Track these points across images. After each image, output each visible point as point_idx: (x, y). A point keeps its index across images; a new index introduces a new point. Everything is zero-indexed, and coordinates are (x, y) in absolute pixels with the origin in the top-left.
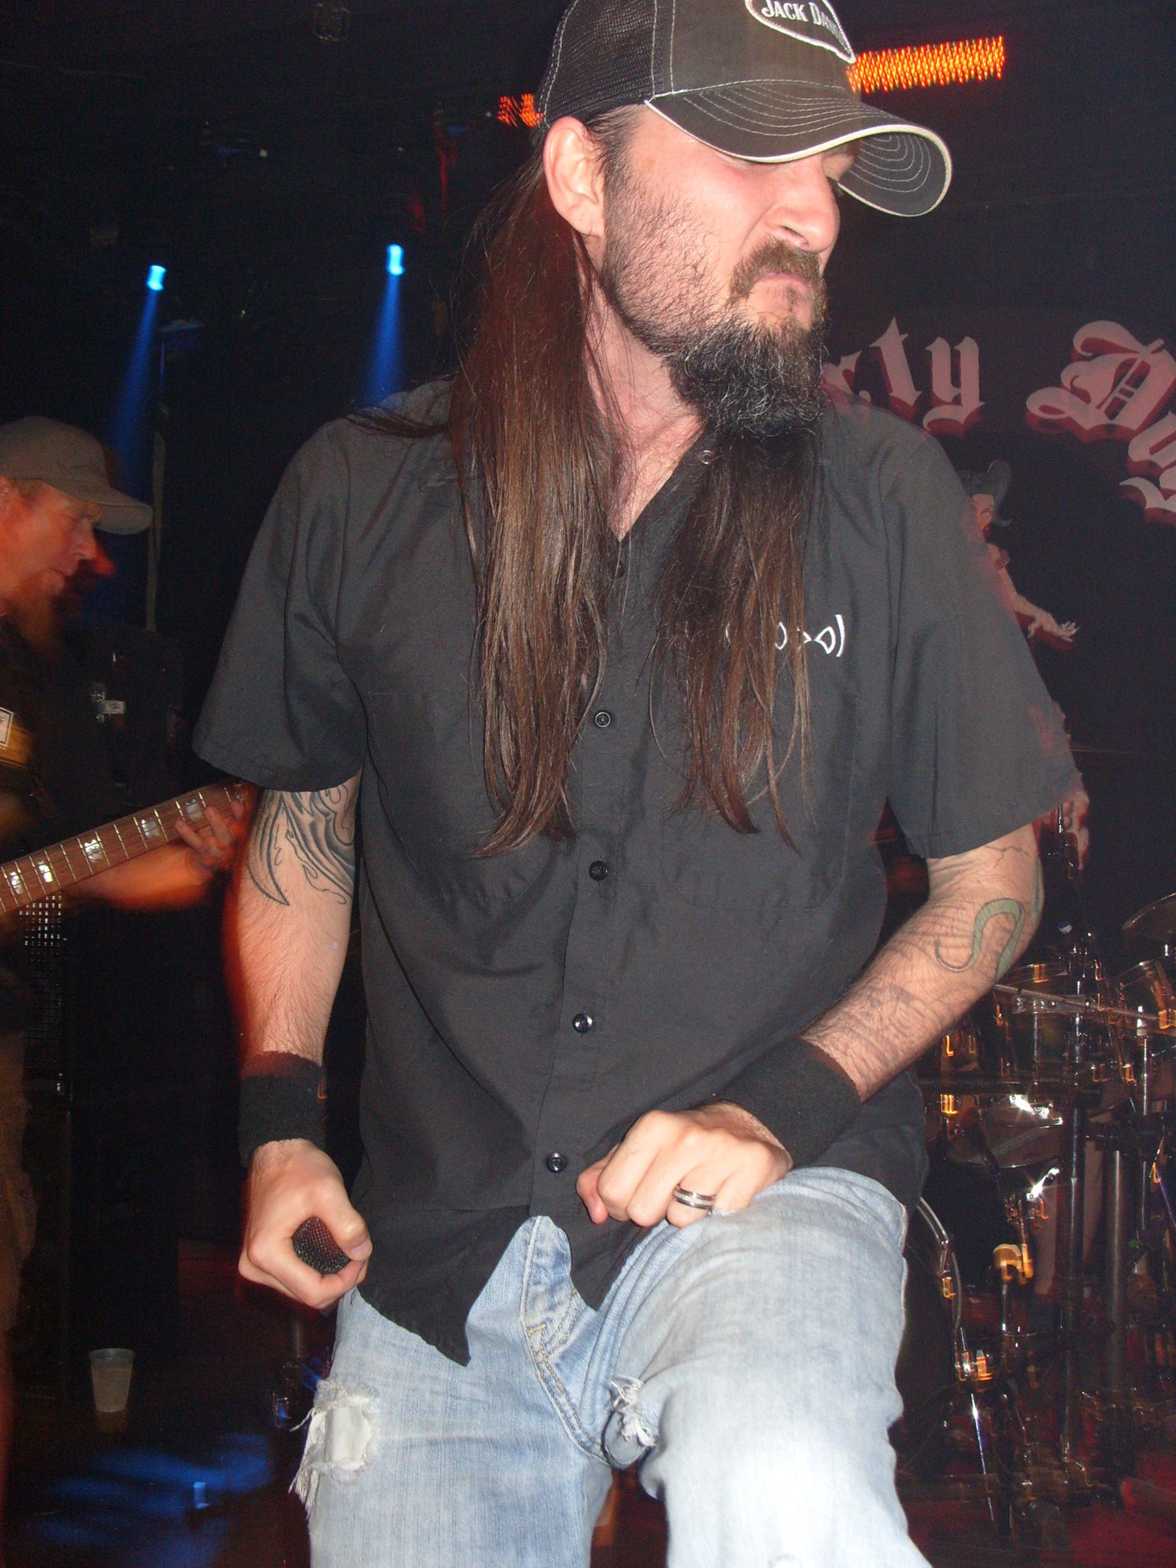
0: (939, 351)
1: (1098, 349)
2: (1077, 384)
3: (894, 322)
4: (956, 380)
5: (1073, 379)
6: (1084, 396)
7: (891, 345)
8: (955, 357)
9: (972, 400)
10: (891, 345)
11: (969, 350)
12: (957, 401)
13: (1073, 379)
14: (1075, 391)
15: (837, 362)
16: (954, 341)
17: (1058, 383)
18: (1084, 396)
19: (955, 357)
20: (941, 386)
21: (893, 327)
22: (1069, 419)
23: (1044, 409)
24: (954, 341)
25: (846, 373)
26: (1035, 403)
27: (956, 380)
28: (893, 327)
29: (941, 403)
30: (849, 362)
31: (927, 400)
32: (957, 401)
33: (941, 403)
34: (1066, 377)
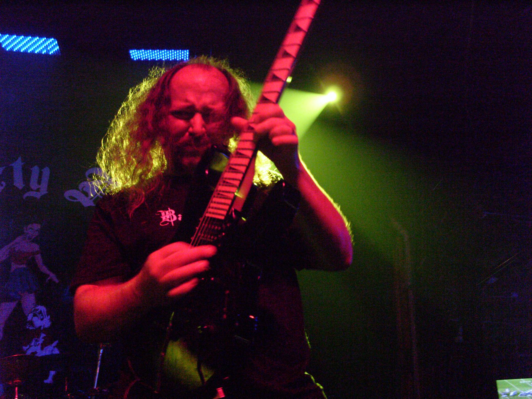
0: (35, 169)
2: (84, 189)
3: (20, 158)
4: (39, 182)
5: (84, 187)
7: (18, 165)
8: (41, 174)
9: (44, 190)
11: (46, 172)
12: (38, 190)
13: (84, 187)
16: (41, 167)
17: (77, 188)
19: (41, 174)
20: (33, 184)
21: (20, 158)
22: (79, 203)
24: (41, 167)
26: (68, 194)
27: (39, 182)
29: (32, 190)
31: (27, 188)
33: (32, 190)
34: (80, 186)
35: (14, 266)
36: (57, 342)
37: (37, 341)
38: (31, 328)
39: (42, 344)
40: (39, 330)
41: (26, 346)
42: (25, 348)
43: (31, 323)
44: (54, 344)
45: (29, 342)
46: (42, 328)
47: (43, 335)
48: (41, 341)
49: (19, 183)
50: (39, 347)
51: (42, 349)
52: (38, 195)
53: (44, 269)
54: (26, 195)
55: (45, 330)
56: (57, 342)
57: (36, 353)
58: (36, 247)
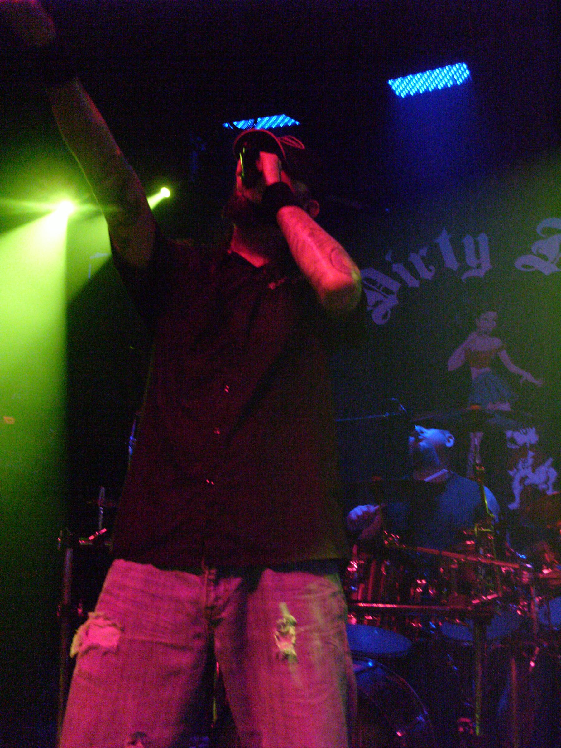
0: (468, 241)
1: (550, 232)
6: (545, 258)
9: (486, 265)
10: (443, 240)
11: (483, 239)
14: (539, 255)
15: (417, 253)
17: (531, 253)
18: (545, 258)
19: (476, 243)
20: (471, 260)
21: (444, 231)
23: (524, 266)
25: (423, 258)
28: (444, 231)
30: (423, 252)
31: (464, 267)
32: (479, 266)
33: (472, 268)
34: (534, 248)
35: (475, 372)
36: (551, 460)
37: (524, 462)
38: (514, 447)
39: (532, 466)
40: (523, 449)
41: (511, 470)
42: (511, 473)
43: (513, 440)
44: (549, 462)
45: (514, 466)
46: (528, 445)
47: (531, 453)
48: (530, 461)
49: (451, 262)
50: (530, 468)
51: (534, 471)
52: (481, 273)
53: (514, 369)
54: (464, 277)
55: (532, 447)
56: (551, 460)
57: (526, 477)
58: (496, 342)
